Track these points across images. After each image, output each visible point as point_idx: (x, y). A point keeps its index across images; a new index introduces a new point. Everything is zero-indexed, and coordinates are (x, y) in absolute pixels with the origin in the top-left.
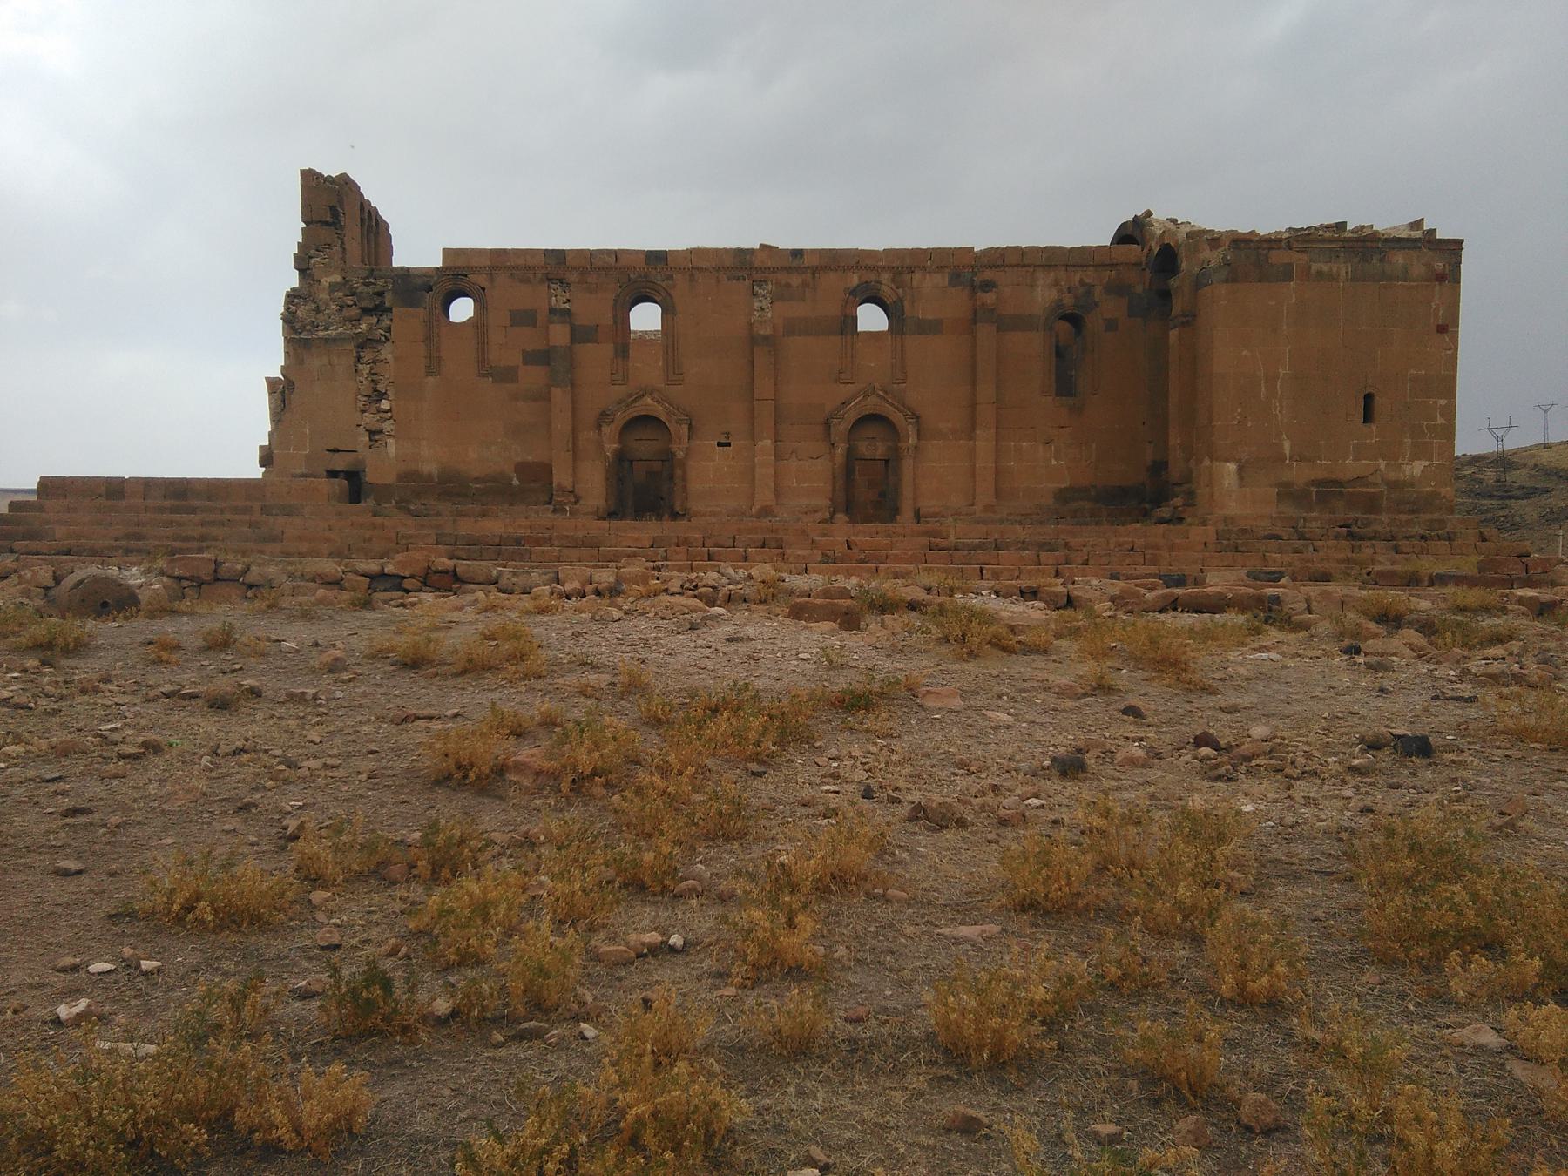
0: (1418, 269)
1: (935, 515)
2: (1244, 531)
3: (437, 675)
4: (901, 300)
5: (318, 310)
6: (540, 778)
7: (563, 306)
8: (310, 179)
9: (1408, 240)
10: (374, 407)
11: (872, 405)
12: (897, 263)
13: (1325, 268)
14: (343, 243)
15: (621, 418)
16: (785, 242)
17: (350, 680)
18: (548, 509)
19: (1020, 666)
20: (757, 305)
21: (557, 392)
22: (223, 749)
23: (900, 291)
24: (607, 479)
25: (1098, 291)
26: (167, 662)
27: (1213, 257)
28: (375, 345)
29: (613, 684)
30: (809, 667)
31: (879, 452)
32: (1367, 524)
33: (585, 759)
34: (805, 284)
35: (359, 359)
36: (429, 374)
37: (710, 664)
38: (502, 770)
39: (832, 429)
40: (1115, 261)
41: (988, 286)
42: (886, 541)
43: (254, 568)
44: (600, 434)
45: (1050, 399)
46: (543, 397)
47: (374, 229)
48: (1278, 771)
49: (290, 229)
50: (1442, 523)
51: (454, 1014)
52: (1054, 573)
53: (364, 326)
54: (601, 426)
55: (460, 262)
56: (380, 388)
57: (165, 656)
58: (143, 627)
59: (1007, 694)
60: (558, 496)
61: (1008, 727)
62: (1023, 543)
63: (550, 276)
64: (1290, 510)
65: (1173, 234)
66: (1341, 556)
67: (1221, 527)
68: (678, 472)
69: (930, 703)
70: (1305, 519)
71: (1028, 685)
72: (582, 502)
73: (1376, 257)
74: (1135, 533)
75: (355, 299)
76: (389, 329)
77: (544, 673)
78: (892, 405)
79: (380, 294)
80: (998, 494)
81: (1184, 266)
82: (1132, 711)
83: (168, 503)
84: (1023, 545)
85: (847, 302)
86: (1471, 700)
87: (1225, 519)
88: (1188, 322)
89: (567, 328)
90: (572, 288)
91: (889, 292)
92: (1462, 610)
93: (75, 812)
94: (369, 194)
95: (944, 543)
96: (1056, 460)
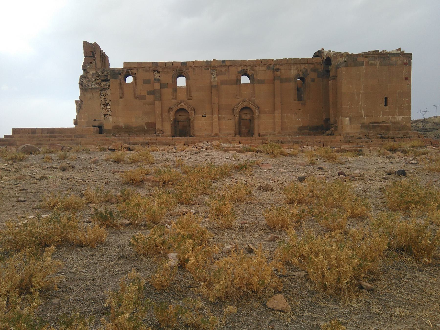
0: (399, 62)
1: (264, 135)
2: (352, 137)
3: (124, 164)
4: (253, 74)
5: (89, 81)
6: (154, 183)
7: (158, 78)
8: (86, 45)
9: (396, 54)
10: (105, 107)
11: (245, 104)
13: (373, 62)
14: (96, 62)
15: (175, 109)
16: (220, 59)
17: (100, 165)
19: (288, 159)
20: (213, 76)
21: (157, 102)
22: (64, 178)
24: (171, 127)
25: (309, 70)
26: (48, 162)
27: (341, 60)
28: (105, 90)
29: (174, 165)
30: (229, 161)
31: (248, 117)
32: (386, 134)
33: (166, 177)
34: (226, 70)
35: (101, 94)
36: (121, 98)
37: (201, 160)
38: (143, 181)
39: (235, 111)
40: (313, 62)
41: (278, 70)
42: (250, 141)
43: (72, 148)
44: (169, 114)
46: (153, 104)
47: (104, 58)
48: (362, 180)
49: (81, 59)
50: (407, 133)
51: (130, 224)
53: (102, 85)
55: (129, 66)
56: (107, 102)
57: (48, 160)
58: (41, 156)
59: (285, 165)
60: (158, 132)
61: (285, 173)
62: (289, 141)
63: (154, 70)
64: (364, 131)
65: (330, 54)
66: (379, 143)
67: (345, 136)
68: (192, 124)
69: (263, 168)
70: (369, 133)
71: (291, 163)
73: (387, 59)
74: (320, 138)
75: (99, 77)
76: (109, 86)
77: (154, 162)
78: (251, 104)
79: (106, 76)
80: (282, 129)
81: (333, 63)
82: (320, 168)
83: (48, 135)
84: (289, 142)
86: (417, 164)
87: (346, 133)
88: (334, 78)
89: (159, 84)
90: (160, 73)
91: (250, 72)
92: (414, 147)
93: (23, 190)
94: (102, 48)
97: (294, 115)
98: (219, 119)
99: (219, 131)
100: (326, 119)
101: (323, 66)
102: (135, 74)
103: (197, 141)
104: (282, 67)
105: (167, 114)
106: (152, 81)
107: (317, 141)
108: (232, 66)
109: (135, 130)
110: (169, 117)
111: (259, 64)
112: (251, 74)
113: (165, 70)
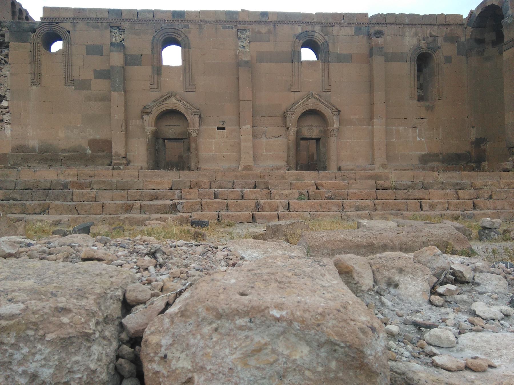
11: (311, 104)
12: (323, 21)
15: (156, 111)
18: (108, 169)
20: (240, 44)
23: (326, 37)
24: (148, 150)
31: (315, 134)
34: (269, 32)
36: (33, 84)
39: (288, 119)
41: (379, 34)
45: (415, 102)
46: (106, 99)
52: (472, 206)
54: (143, 116)
60: (115, 160)
62: (442, 183)
68: (193, 145)
72: (132, 164)
76: (7, 56)
80: (388, 158)
84: (443, 186)
85: (295, 43)
89: (121, 55)
90: (126, 32)
95: (387, 184)
96: (419, 138)
97: (410, 130)
98: (255, 136)
99: (254, 160)
100: (477, 139)
101: (469, 29)
102: (69, 32)
103: (206, 180)
104: (384, 29)
105: (138, 122)
106: (106, 49)
107: (508, 185)
108: (282, 22)
109: (64, 157)
110: (143, 128)
111: (338, 22)
112: (323, 41)
113: (136, 27)
